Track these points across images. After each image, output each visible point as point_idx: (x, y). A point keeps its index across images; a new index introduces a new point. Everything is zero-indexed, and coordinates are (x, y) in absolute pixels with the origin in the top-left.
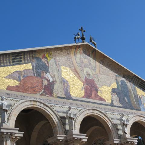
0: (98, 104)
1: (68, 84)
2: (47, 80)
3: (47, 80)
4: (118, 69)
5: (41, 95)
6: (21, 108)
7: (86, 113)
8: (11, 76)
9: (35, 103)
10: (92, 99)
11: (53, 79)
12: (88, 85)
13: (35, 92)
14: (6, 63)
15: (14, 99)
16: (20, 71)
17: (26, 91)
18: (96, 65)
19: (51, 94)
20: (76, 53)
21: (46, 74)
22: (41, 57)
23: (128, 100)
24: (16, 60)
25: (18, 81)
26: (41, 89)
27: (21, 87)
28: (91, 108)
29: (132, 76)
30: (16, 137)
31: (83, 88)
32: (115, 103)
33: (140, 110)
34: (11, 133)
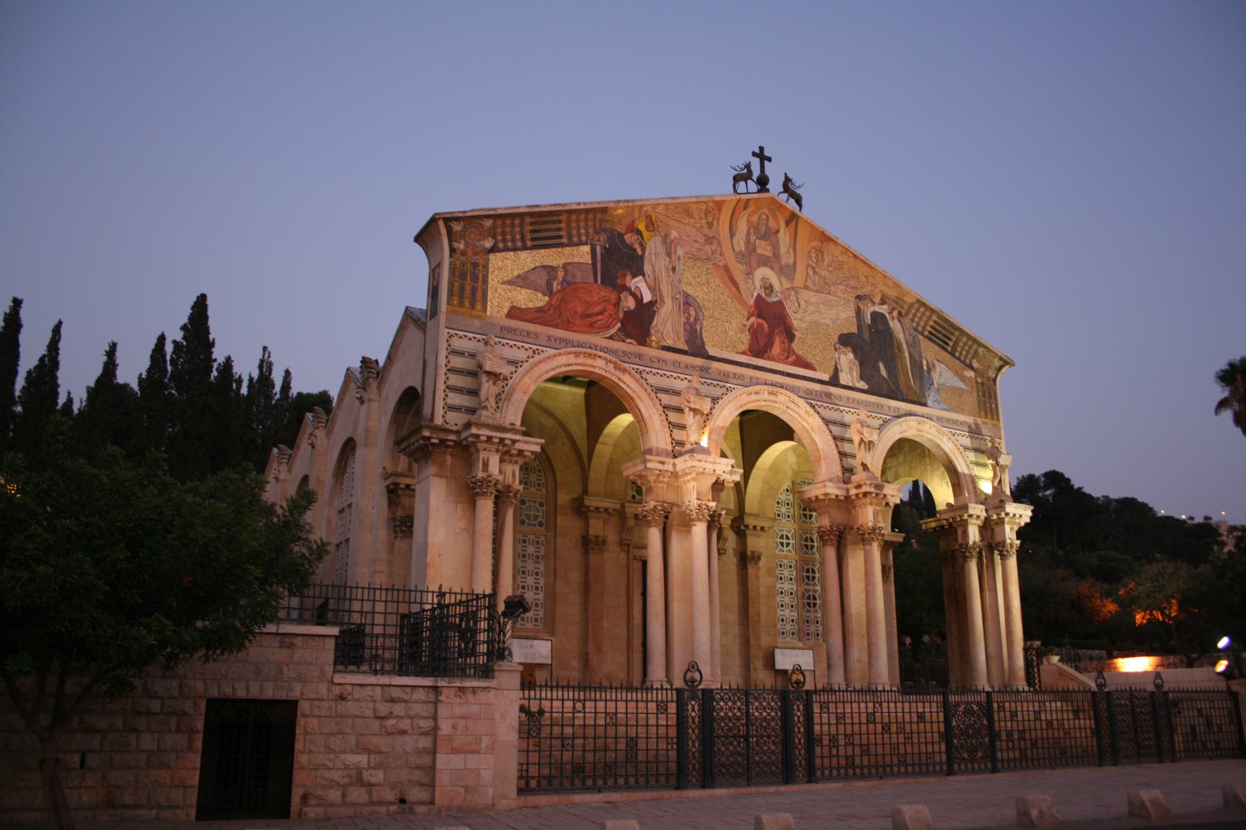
0: (788, 375)
1: (699, 308)
2: (634, 295)
3: (634, 295)
4: (867, 277)
5: (611, 338)
6: (546, 373)
8: (522, 281)
9: (590, 361)
11: (654, 295)
12: (763, 318)
13: (592, 328)
14: (513, 240)
15: (527, 346)
16: (552, 267)
17: (568, 326)
18: (795, 262)
19: (642, 337)
20: (733, 222)
21: (634, 276)
22: (621, 228)
23: (889, 372)
25: (544, 294)
27: (551, 312)
29: (910, 300)
30: (521, 452)
31: (748, 327)
32: (844, 378)
33: (925, 405)
34: (502, 440)
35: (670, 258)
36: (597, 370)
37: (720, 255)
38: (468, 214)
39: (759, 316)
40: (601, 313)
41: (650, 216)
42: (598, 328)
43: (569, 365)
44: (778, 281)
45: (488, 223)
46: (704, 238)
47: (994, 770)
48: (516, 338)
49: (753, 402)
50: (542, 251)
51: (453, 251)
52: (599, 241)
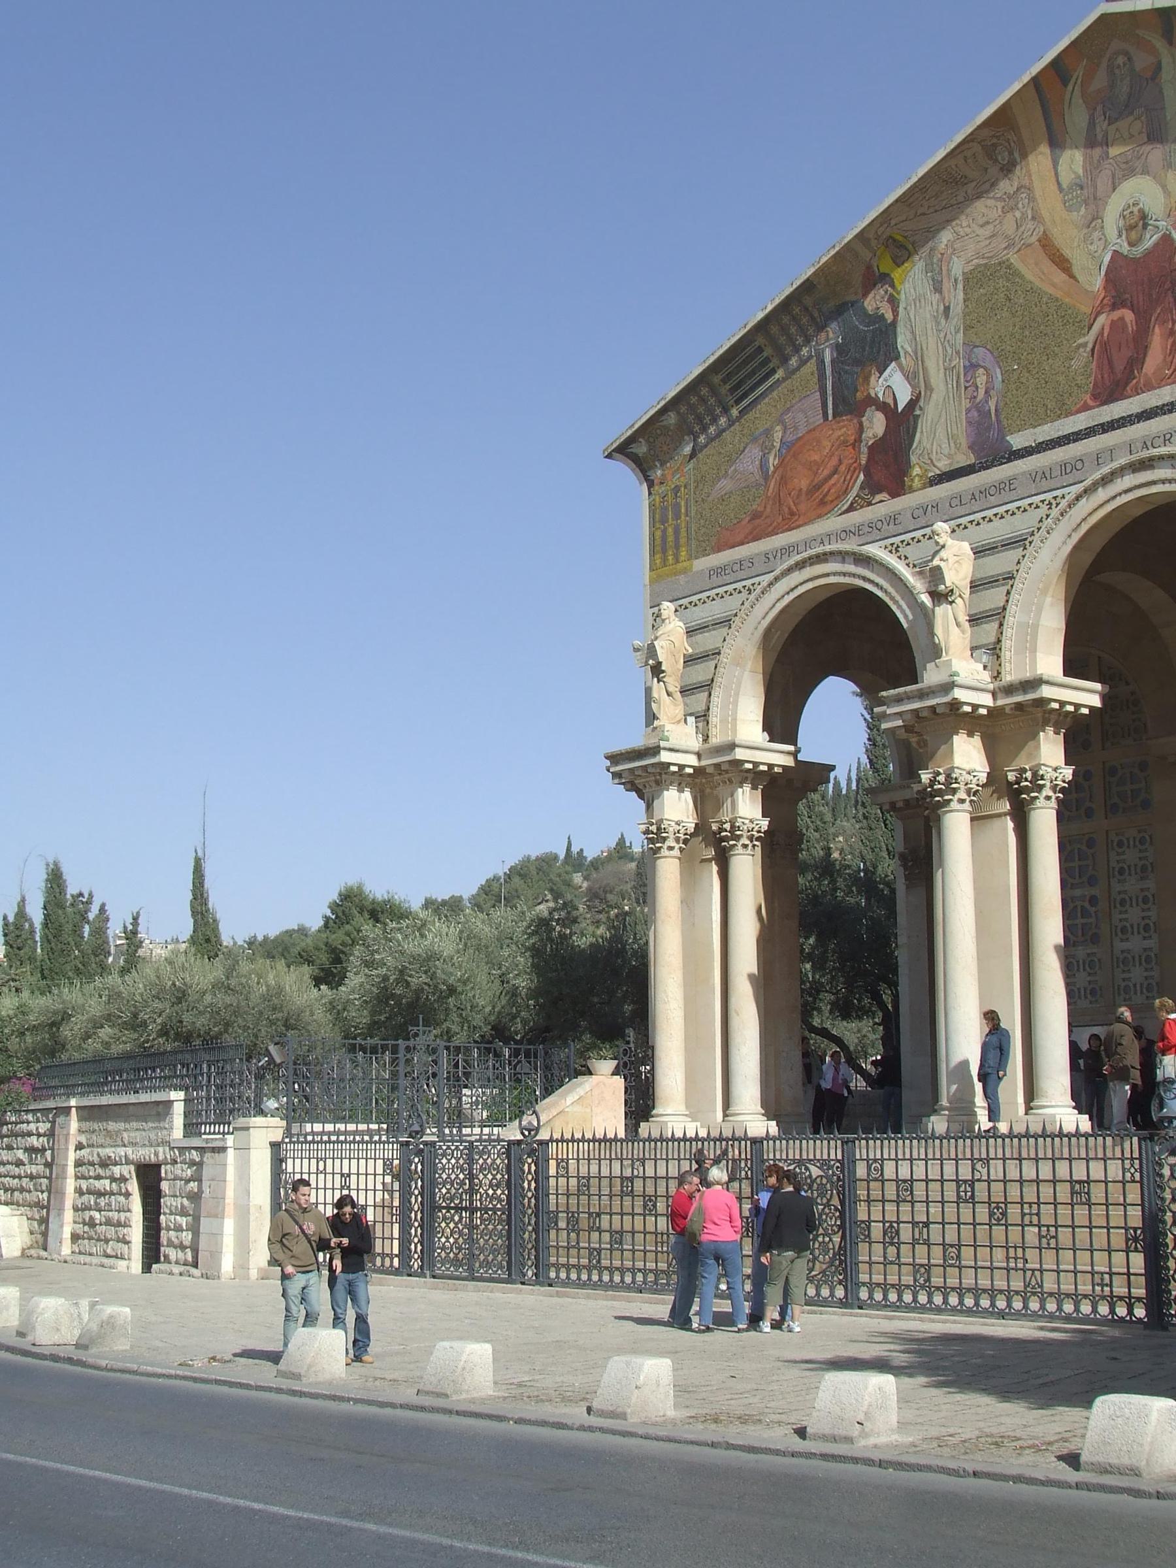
3: (883, 407)
5: (851, 509)
6: (764, 618)
7: (1085, 505)
10: (1149, 387)
12: (1123, 304)
13: (823, 506)
15: (739, 585)
17: (790, 522)
21: (881, 374)
24: (746, 387)
26: (854, 471)
27: (768, 510)
28: (1123, 461)
31: (1090, 346)
35: (940, 292)
36: (832, 580)
37: (1033, 218)
38: (636, 426)
39: (1114, 307)
40: (835, 472)
41: (891, 237)
42: (832, 501)
43: (792, 590)
44: (1158, 190)
45: (672, 419)
46: (1000, 205)
47: (850, 1302)
48: (728, 579)
49: (1101, 505)
50: (750, 415)
51: (651, 485)
52: (827, 339)
